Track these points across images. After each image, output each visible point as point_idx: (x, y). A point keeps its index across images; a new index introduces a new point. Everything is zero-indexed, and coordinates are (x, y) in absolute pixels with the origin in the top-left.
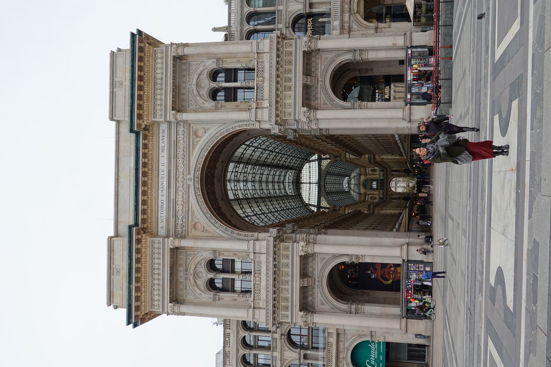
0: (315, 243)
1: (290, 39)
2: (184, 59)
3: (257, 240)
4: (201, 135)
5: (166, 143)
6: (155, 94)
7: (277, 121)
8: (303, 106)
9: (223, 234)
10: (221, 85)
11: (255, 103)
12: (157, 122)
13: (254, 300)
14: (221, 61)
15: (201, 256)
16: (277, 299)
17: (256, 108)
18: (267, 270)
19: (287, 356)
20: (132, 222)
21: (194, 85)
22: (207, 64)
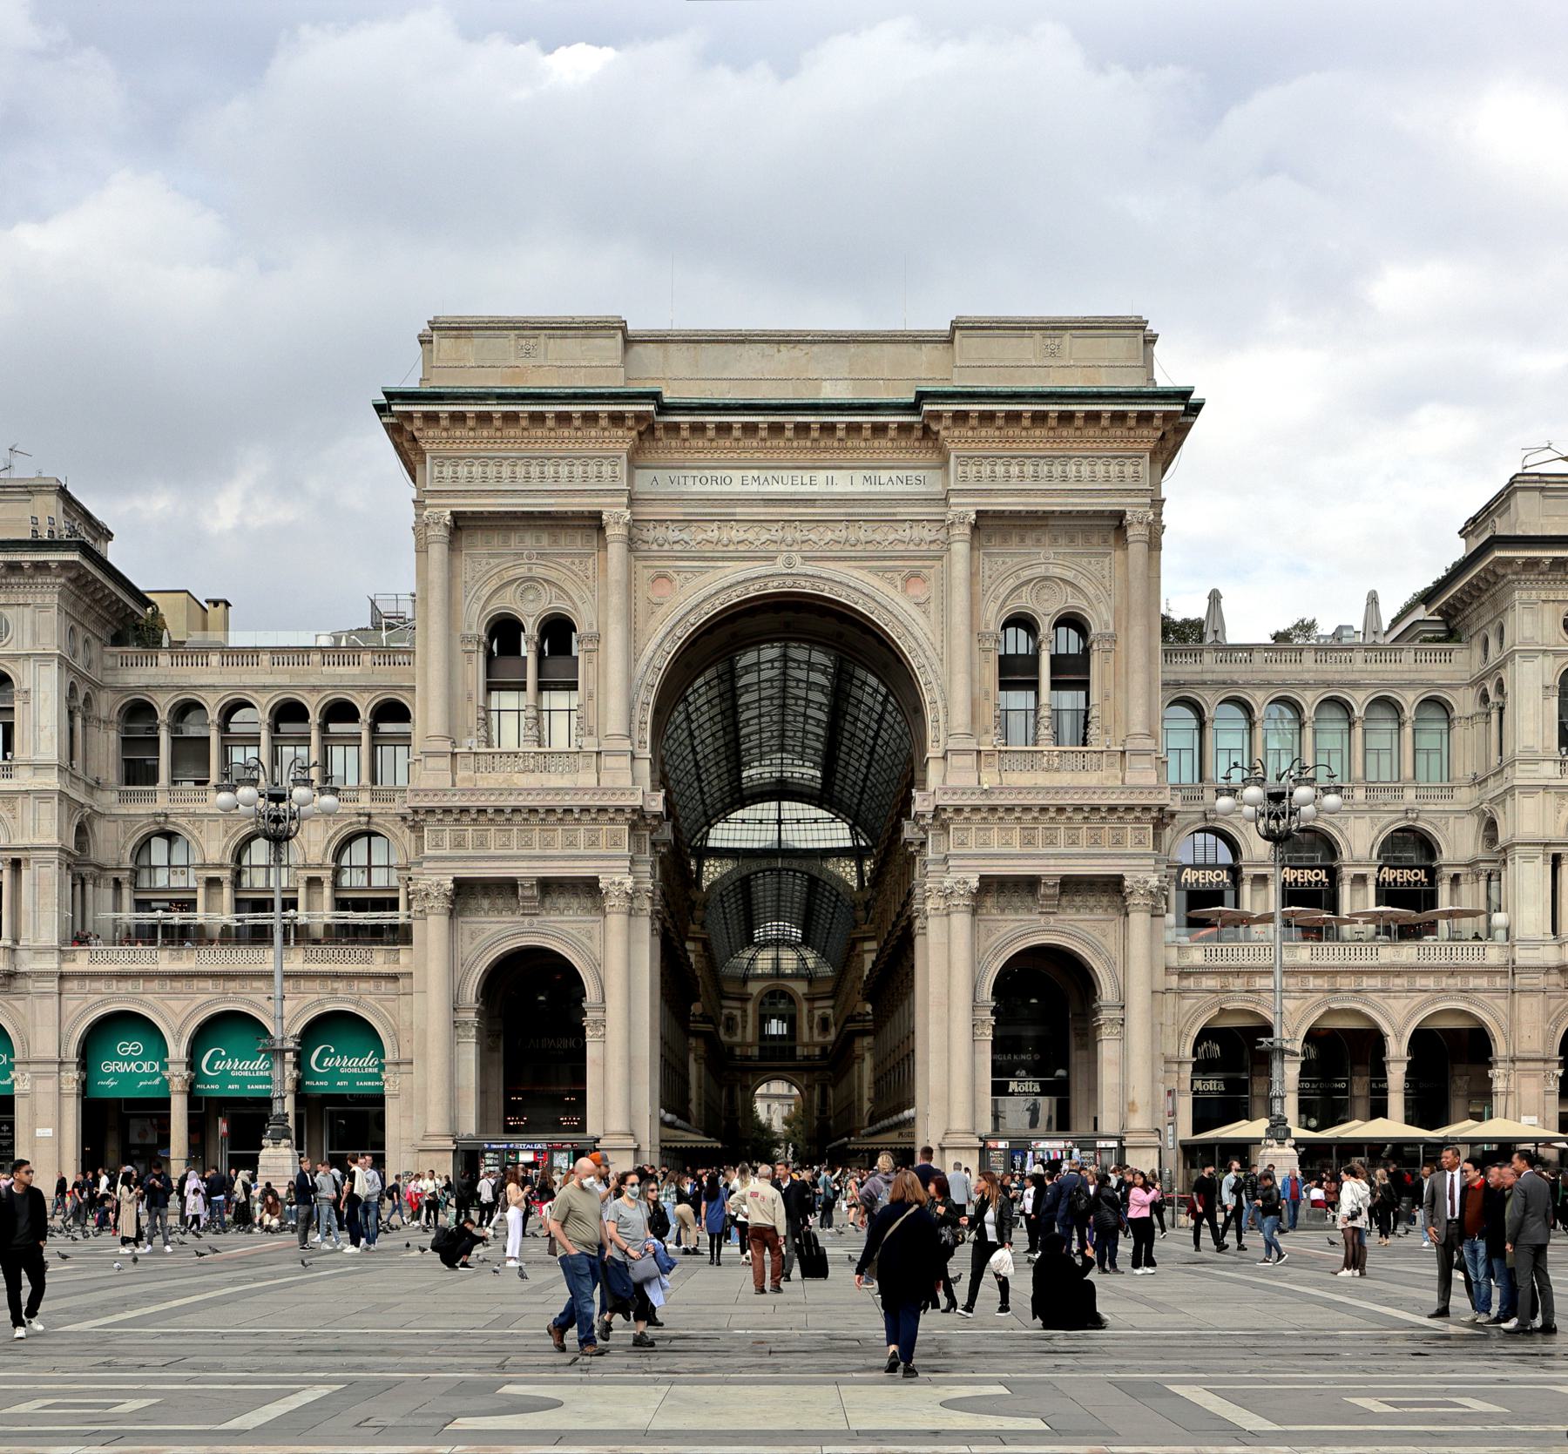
0: (630, 915)
1: (1157, 837)
2: (1117, 540)
3: (633, 758)
4: (911, 591)
5: (890, 488)
6: (1022, 459)
7: (945, 810)
8: (982, 877)
9: (644, 660)
10: (1044, 646)
11: (991, 748)
12: (947, 462)
13: (475, 753)
14: (1107, 646)
15: (581, 598)
16: (482, 818)
17: (979, 752)
18: (558, 791)
19: (312, 831)
20: (668, 397)
21: (1047, 569)
22: (1102, 608)
